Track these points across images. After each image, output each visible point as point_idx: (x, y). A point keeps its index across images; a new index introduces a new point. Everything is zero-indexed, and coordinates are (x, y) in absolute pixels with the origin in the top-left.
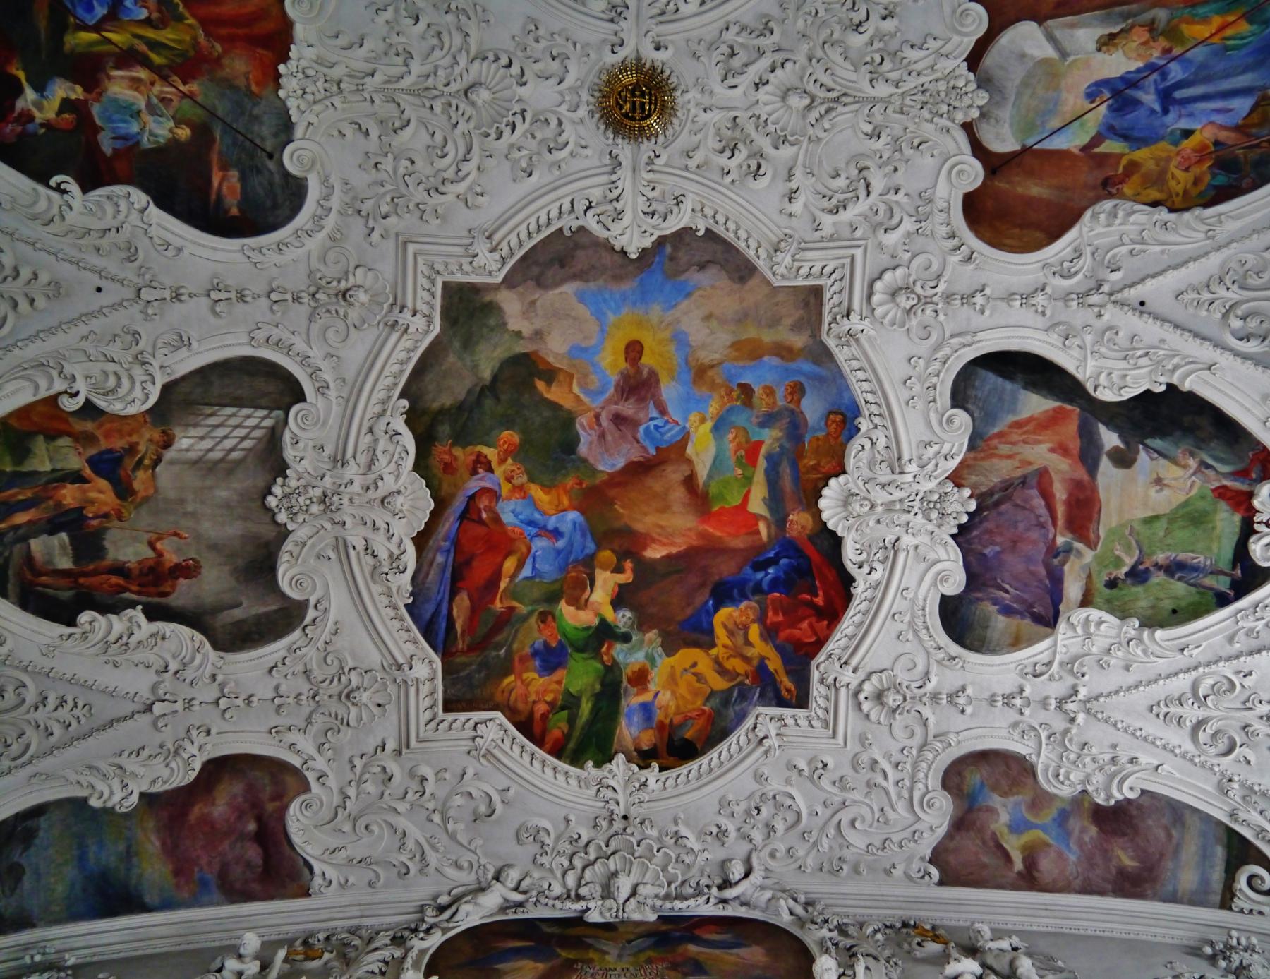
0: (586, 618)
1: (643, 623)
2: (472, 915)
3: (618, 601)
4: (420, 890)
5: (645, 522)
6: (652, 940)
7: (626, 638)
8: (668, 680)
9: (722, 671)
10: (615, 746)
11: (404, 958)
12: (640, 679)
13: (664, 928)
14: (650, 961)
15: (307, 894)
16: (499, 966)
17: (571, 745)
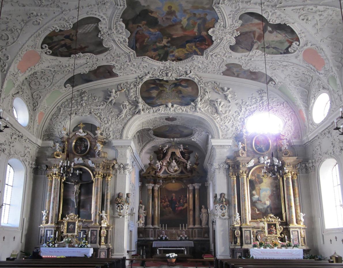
0: (162, 45)
1: (172, 45)
2: (145, 80)
3: (168, 42)
4: (136, 75)
5: (172, 32)
6: (174, 85)
7: (169, 47)
8: (177, 53)
9: (187, 51)
10: (168, 59)
11: (136, 91)
12: (172, 52)
13: (176, 82)
14: (173, 91)
15: (118, 76)
16: (151, 92)
17: (160, 59)
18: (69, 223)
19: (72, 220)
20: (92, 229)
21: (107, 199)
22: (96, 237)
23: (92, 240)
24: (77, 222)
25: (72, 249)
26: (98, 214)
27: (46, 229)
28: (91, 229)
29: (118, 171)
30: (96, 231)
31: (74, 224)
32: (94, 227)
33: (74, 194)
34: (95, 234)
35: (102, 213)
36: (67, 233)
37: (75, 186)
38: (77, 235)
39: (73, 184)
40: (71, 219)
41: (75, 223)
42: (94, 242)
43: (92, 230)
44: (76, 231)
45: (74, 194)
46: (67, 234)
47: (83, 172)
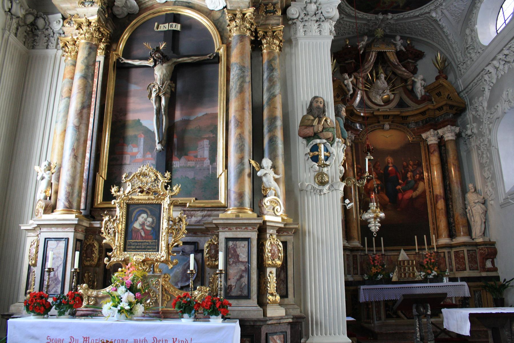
18: (131, 209)
19: (148, 193)
20: (230, 235)
21: (273, 119)
22: (248, 271)
23: (232, 282)
24: (166, 203)
25: (149, 329)
26: (247, 171)
27: (45, 234)
28: (223, 236)
29: (300, 26)
30: (246, 243)
31: (155, 209)
32: (238, 226)
33: (154, 95)
34: (243, 257)
35: (261, 167)
36: (125, 250)
37: (156, 68)
38: (166, 262)
39: (150, 63)
40: (142, 192)
41: (159, 206)
42: (239, 293)
43: (227, 240)
44: (163, 244)
45: (154, 95)
46: (127, 254)
47: (182, 27)
